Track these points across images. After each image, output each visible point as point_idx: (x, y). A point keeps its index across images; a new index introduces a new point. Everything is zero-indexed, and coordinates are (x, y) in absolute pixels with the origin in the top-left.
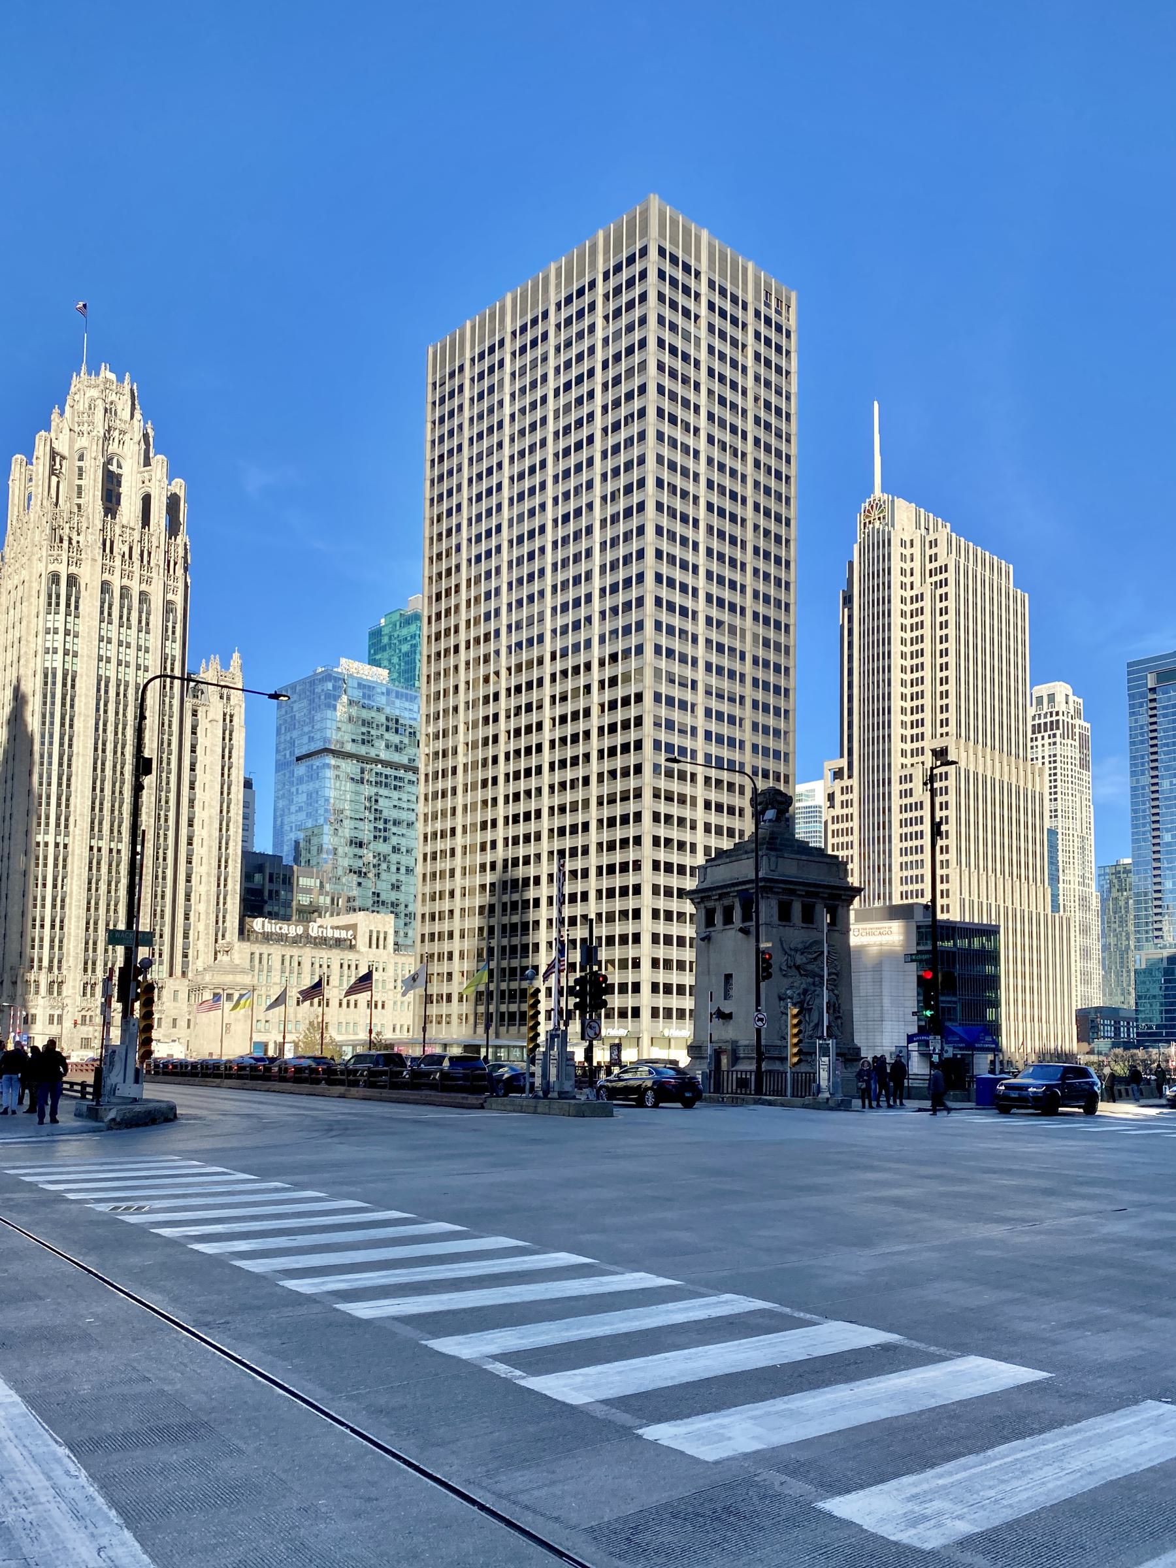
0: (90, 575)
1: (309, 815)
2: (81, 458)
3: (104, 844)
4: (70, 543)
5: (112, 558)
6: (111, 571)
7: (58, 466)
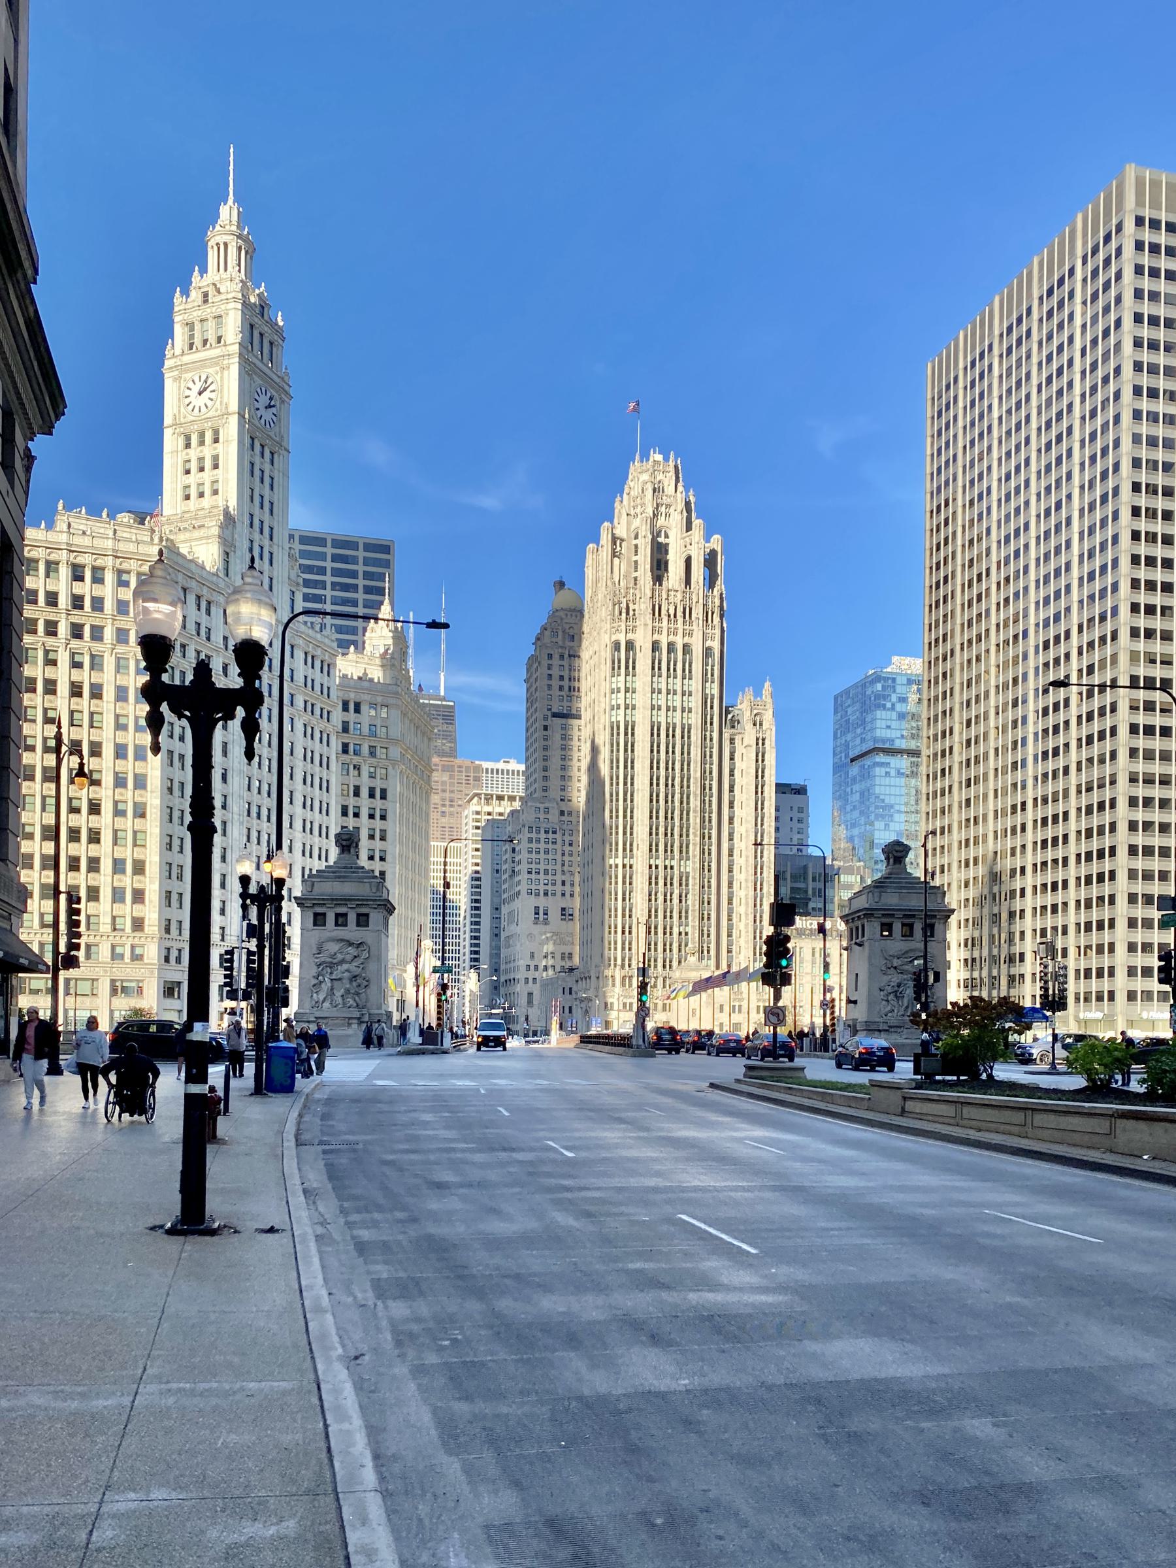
0: (643, 640)
1: (862, 813)
2: (636, 537)
3: (660, 862)
4: (628, 613)
5: (660, 620)
6: (660, 632)
7: (618, 549)
